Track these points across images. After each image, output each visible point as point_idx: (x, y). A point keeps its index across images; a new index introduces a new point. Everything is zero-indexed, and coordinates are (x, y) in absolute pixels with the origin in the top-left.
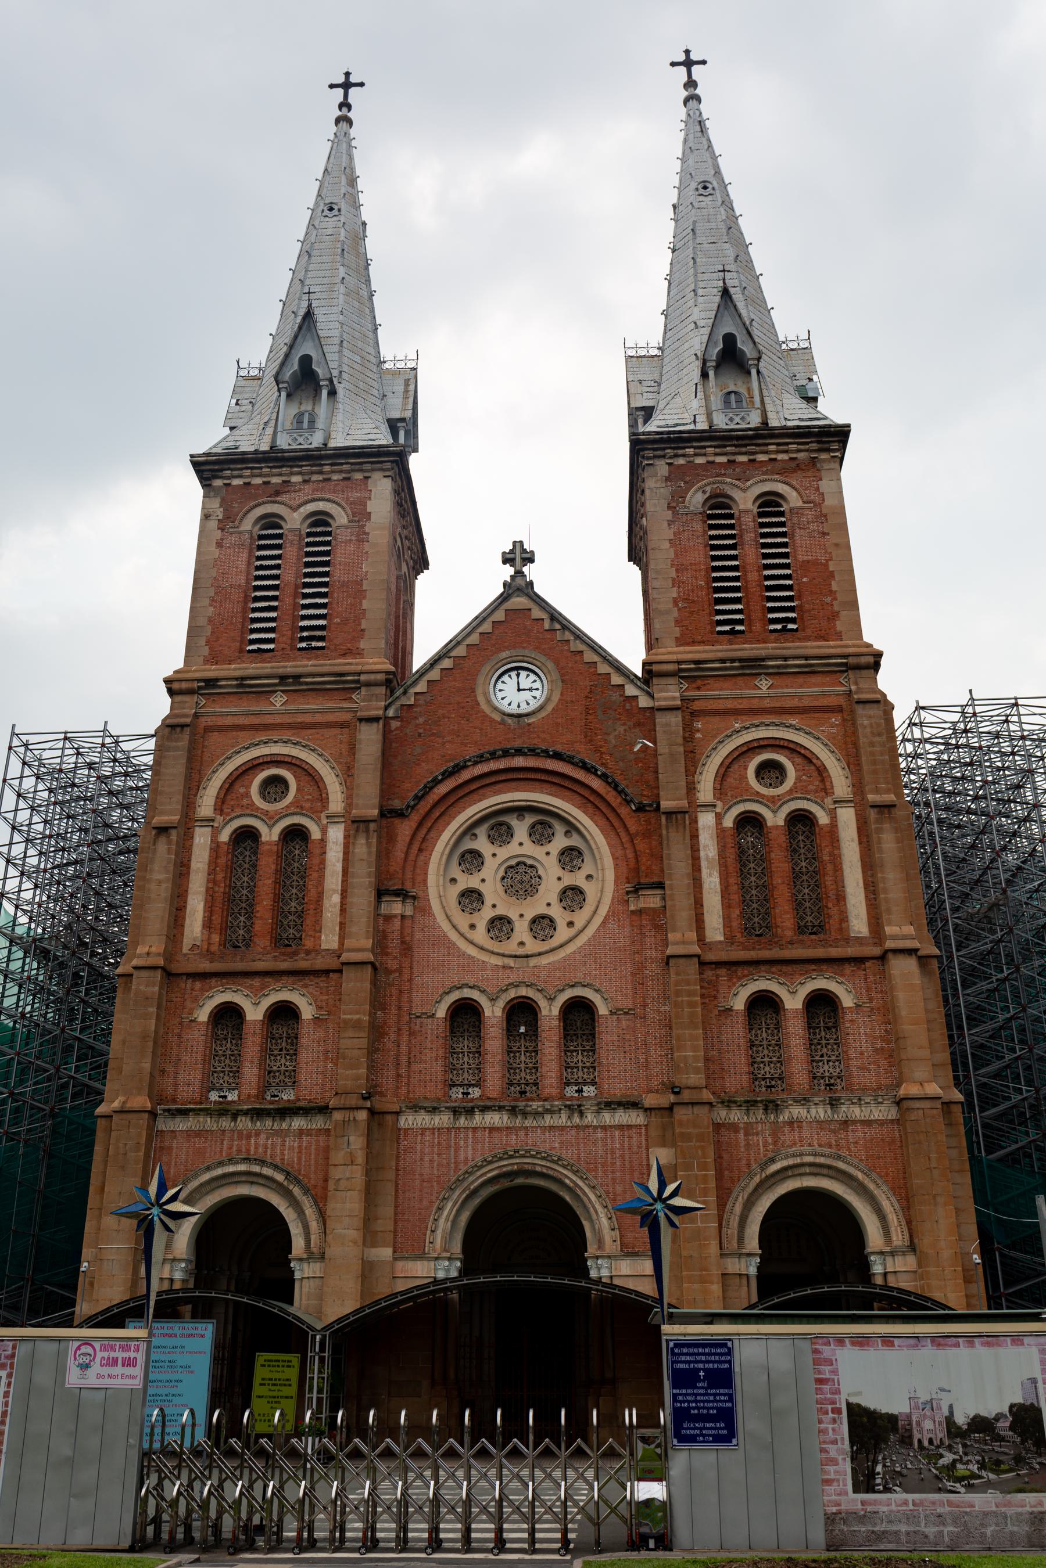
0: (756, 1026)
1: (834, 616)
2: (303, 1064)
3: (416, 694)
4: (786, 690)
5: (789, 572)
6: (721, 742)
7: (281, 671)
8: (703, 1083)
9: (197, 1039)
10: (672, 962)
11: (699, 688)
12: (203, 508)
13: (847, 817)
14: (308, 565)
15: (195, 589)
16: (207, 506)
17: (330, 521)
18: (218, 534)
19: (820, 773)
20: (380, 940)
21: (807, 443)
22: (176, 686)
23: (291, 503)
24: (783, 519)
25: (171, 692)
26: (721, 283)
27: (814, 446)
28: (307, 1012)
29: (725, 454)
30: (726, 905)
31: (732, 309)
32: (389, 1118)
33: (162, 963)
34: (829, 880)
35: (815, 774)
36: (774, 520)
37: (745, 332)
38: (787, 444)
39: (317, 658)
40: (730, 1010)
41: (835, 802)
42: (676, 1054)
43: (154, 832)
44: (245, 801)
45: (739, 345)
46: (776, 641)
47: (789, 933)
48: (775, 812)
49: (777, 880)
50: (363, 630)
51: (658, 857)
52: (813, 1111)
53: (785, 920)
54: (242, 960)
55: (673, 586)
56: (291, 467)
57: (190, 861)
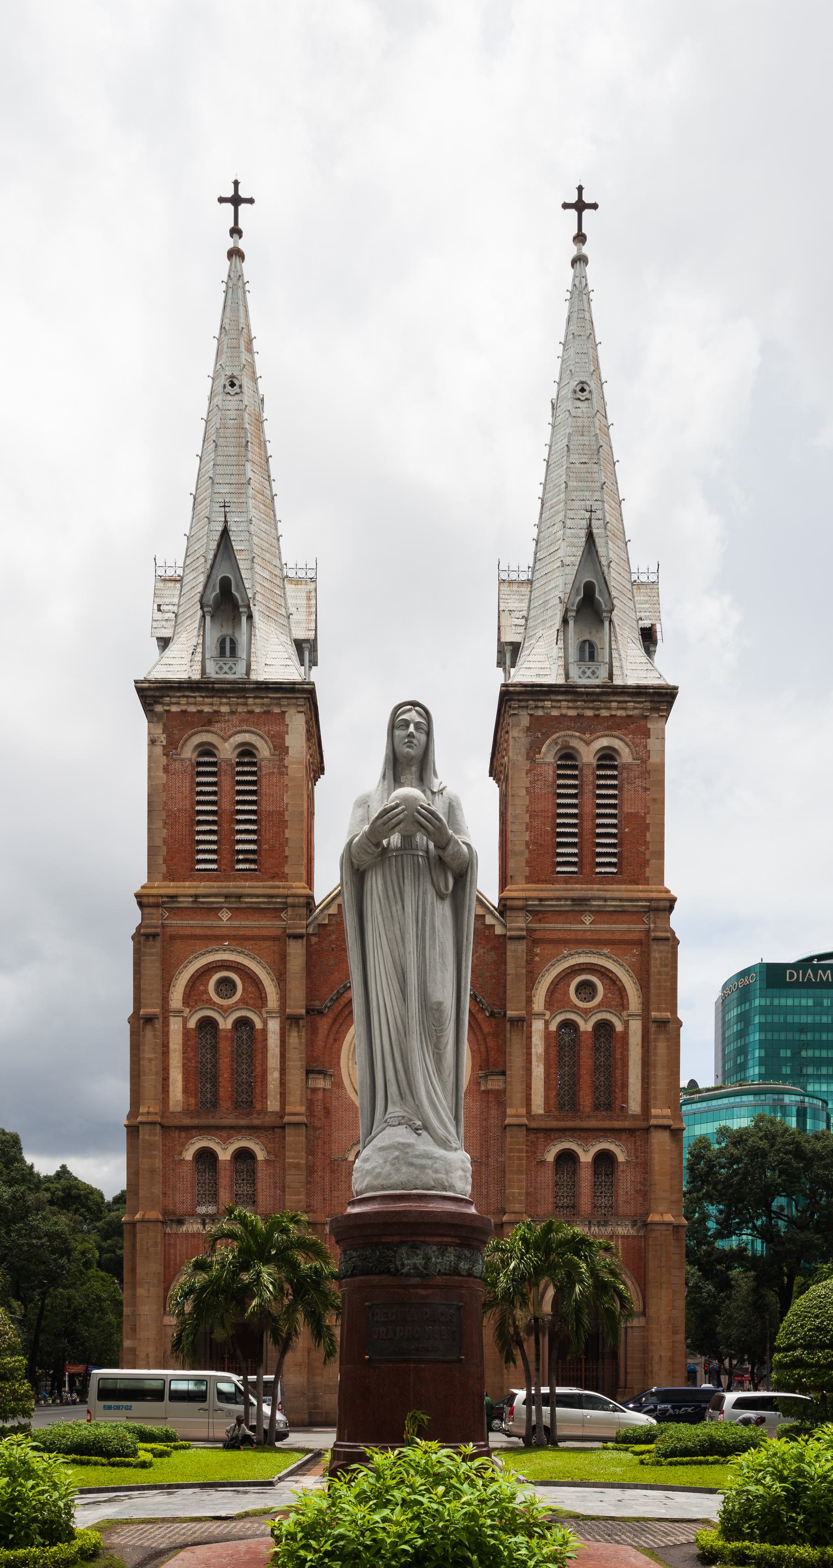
0: (560, 1172)
1: (646, 863)
2: (259, 1190)
3: (330, 915)
4: (602, 926)
5: (614, 821)
6: (552, 965)
7: (225, 891)
8: (524, 1210)
9: (187, 1172)
10: (508, 1129)
11: (540, 921)
12: (149, 734)
13: (636, 1026)
14: (240, 793)
15: (150, 812)
16: (152, 731)
17: (255, 751)
18: (164, 760)
19: (621, 994)
20: (310, 1105)
21: (642, 702)
22: (145, 900)
23: (221, 733)
24: (616, 773)
25: (141, 905)
26: (584, 523)
27: (648, 705)
28: (261, 1155)
29: (576, 708)
30: (547, 1088)
31: (595, 554)
32: (319, 1227)
33: (159, 1120)
34: (618, 1072)
35: (617, 993)
36: (609, 773)
37: (603, 581)
38: (627, 702)
39: (252, 880)
40: (545, 1161)
41: (629, 1015)
42: (507, 1191)
43: (142, 1021)
44: (205, 997)
45: (597, 596)
46: (600, 883)
47: (588, 1109)
48: (586, 1021)
49: (583, 1072)
50: (287, 857)
51: (502, 1051)
52: (592, 1229)
53: (586, 1100)
54: (213, 1117)
55: (527, 831)
56: (220, 697)
57: (168, 1043)
